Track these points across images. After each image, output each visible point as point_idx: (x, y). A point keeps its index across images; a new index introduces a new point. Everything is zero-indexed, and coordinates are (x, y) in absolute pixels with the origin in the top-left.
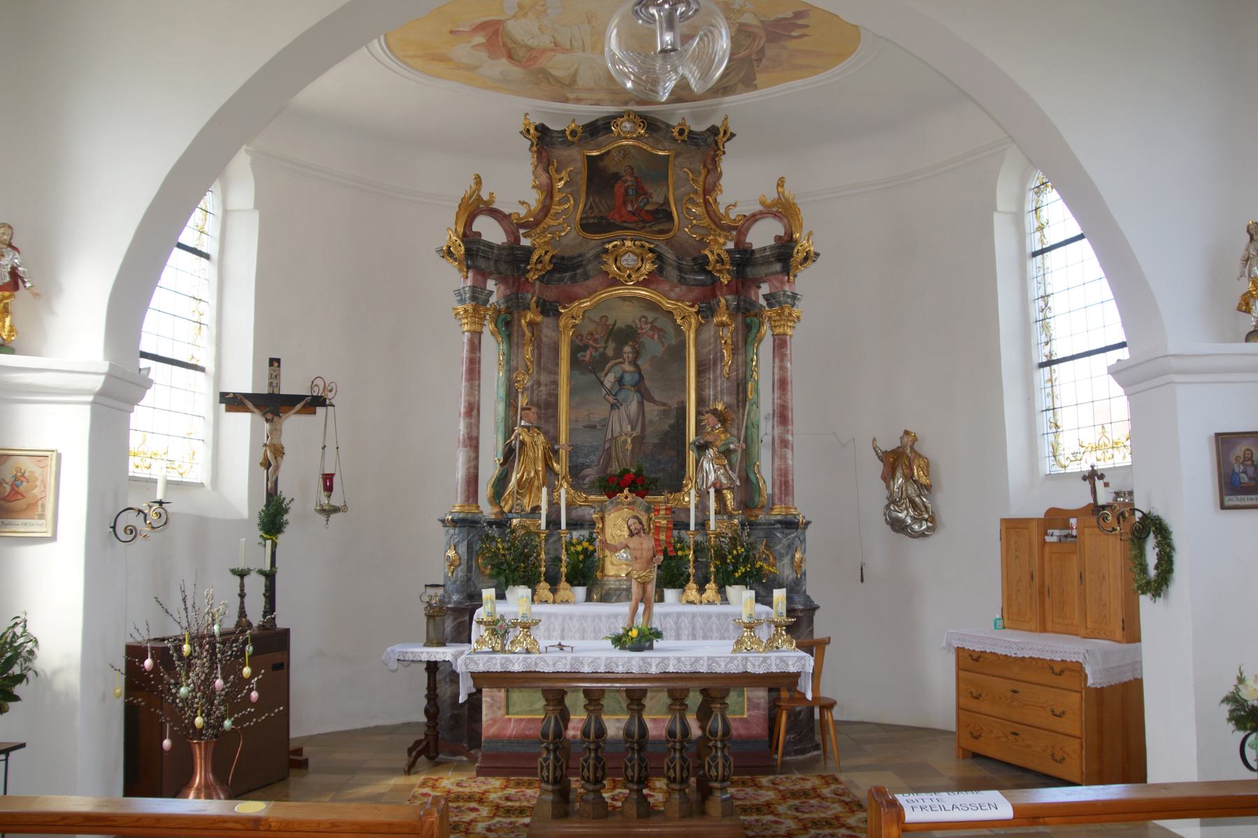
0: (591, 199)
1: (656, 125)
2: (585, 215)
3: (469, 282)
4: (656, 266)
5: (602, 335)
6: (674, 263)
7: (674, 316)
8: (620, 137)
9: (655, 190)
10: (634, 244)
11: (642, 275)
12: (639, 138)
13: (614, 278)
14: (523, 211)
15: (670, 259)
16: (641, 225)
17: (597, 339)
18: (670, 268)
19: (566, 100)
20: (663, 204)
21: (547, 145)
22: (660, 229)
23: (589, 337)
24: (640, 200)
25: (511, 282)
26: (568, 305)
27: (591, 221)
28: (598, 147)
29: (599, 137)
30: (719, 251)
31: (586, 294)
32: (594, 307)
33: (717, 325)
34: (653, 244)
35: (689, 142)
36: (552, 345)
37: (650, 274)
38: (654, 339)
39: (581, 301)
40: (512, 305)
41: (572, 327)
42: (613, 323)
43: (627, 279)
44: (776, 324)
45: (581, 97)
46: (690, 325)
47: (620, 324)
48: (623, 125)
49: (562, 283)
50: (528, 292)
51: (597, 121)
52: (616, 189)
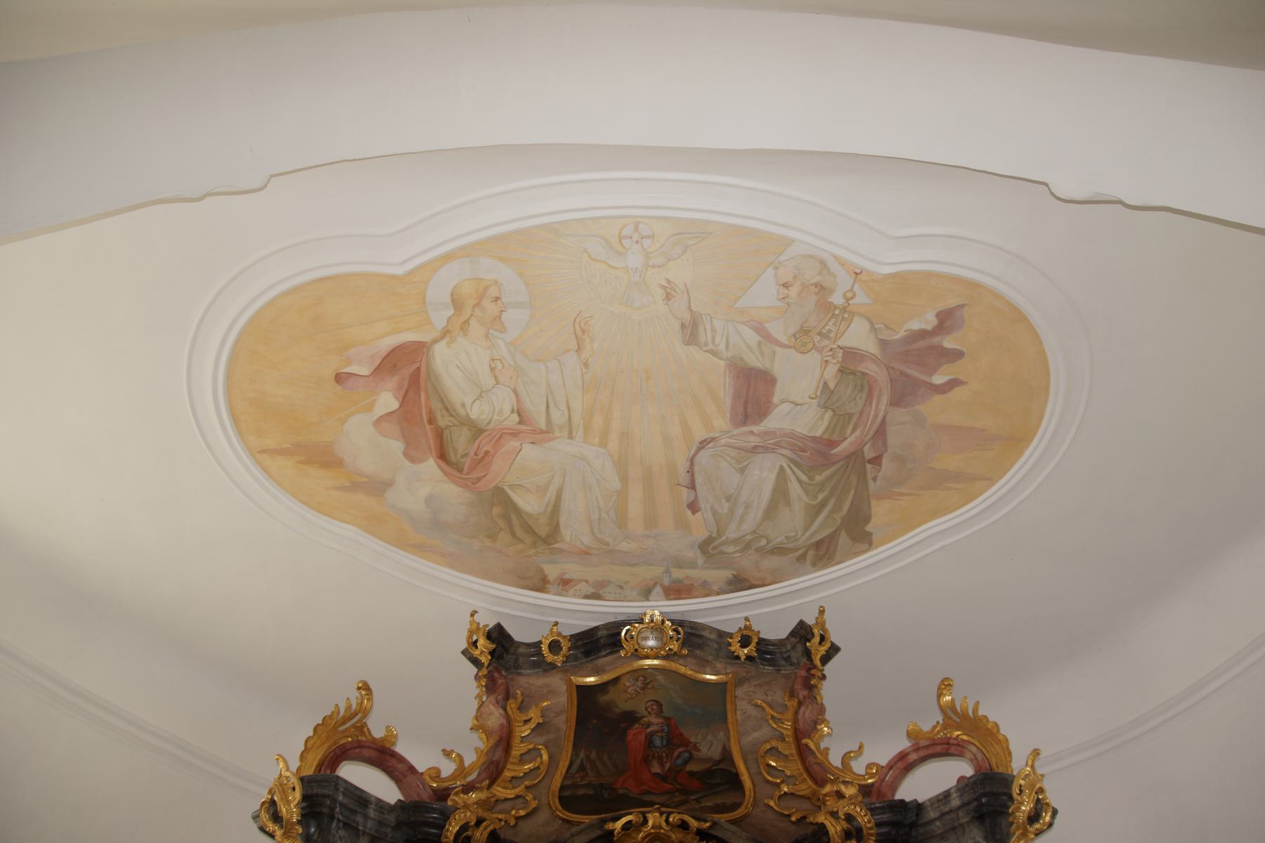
0: (582, 754)
1: (701, 636)
2: (569, 782)
8: (638, 655)
10: (667, 821)
12: (669, 656)
14: (448, 768)
19: (541, 585)
20: (720, 761)
21: (507, 669)
22: (718, 804)
24: (676, 754)
27: (581, 792)
29: (599, 657)
30: (849, 809)
45: (567, 576)
51: (597, 628)
52: (630, 737)
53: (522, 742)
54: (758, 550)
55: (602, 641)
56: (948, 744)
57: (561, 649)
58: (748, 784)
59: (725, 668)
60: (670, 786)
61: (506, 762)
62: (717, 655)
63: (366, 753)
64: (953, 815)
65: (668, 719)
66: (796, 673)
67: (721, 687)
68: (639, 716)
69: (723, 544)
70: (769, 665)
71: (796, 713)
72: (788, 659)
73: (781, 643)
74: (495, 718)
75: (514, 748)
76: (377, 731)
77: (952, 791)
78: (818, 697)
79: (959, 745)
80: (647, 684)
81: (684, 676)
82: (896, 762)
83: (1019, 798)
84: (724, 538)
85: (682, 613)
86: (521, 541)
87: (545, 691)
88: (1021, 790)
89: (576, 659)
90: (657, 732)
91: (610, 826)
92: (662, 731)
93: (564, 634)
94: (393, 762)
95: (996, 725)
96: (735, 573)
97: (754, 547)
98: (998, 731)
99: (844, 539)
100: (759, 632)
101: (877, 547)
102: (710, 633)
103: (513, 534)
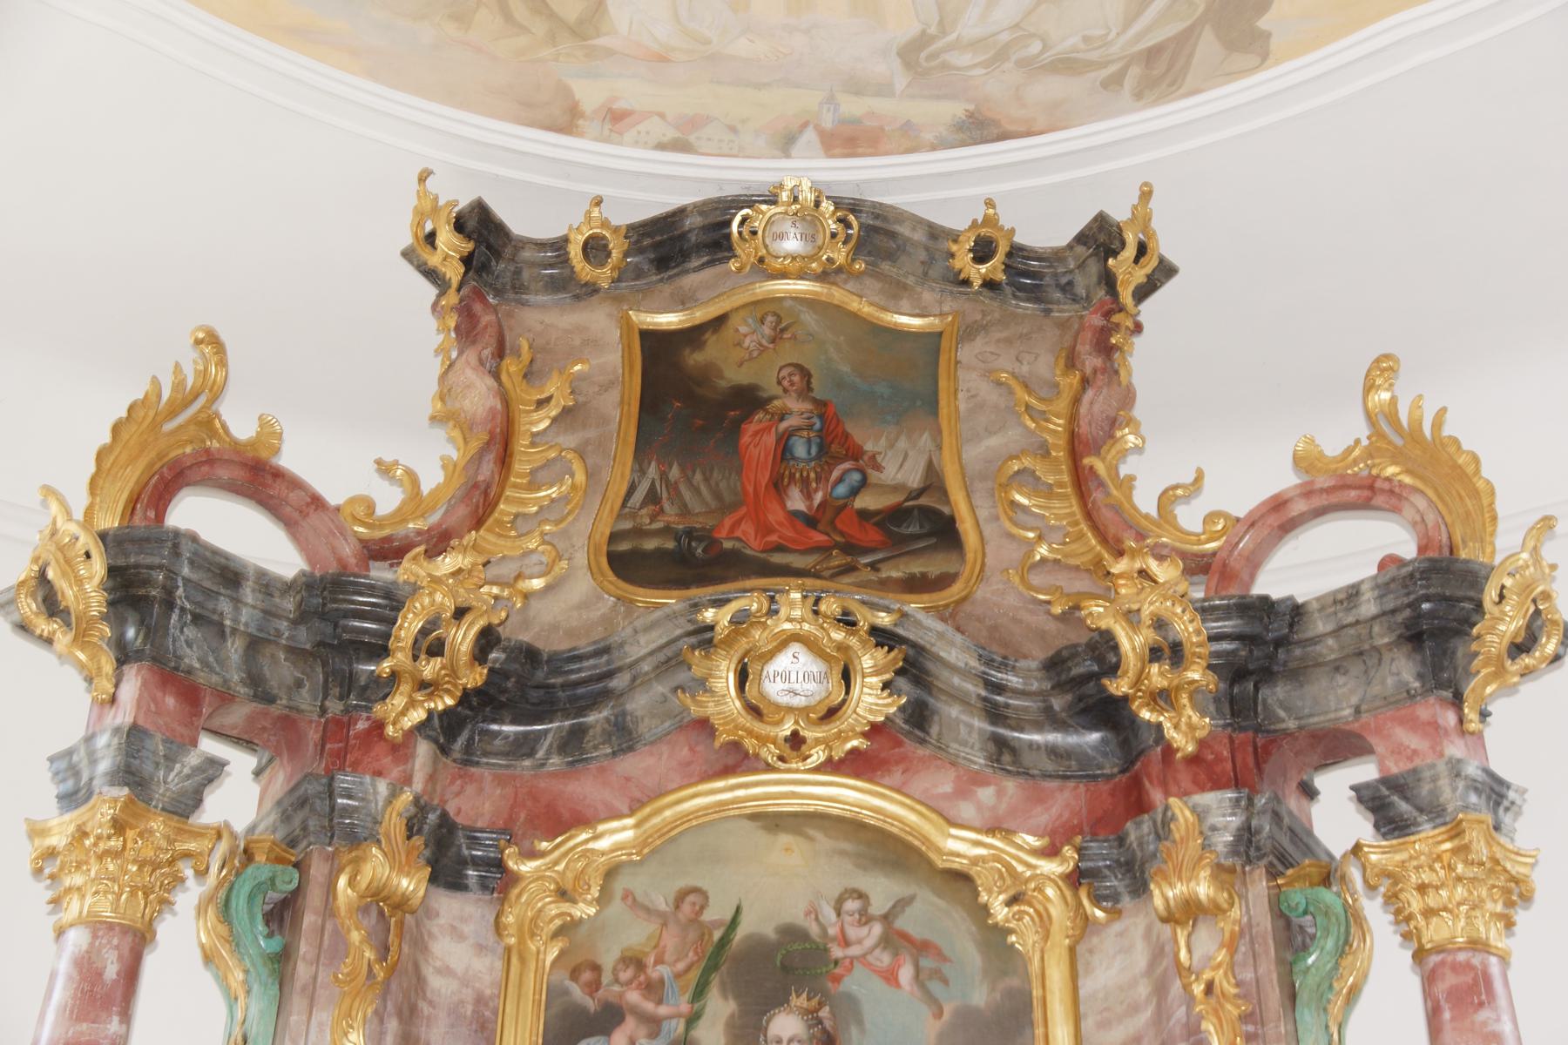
0: (653, 471)
1: (892, 235)
2: (627, 525)
3: (124, 714)
4: (904, 700)
5: (681, 966)
6: (969, 687)
7: (977, 894)
8: (763, 268)
9: (891, 446)
11: (841, 737)
13: (736, 746)
14: (388, 499)
15: (953, 668)
16: (838, 560)
17: (662, 981)
18: (954, 711)
19: (567, 121)
20: (921, 492)
21: (498, 293)
23: (625, 975)
24: (836, 474)
25: (313, 735)
26: (544, 845)
27: (650, 545)
28: (682, 302)
29: (687, 272)
31: (626, 810)
32: (654, 849)
33: (1169, 919)
34: (888, 610)
35: (1008, 290)
36: (469, 1009)
37: (875, 731)
38: (897, 985)
39: (601, 828)
40: (305, 828)
41: (556, 934)
42: (728, 916)
43: (787, 752)
44: (1432, 900)
45: (621, 105)
46: (1044, 920)
47: (758, 923)
48: (776, 229)
49: (527, 763)
50: (379, 773)
51: (680, 213)
52: (745, 439)
53: (533, 445)
54: (1023, 63)
55: (693, 238)
56: (1371, 488)
57: (609, 255)
58: (970, 538)
59: (941, 303)
60: (823, 538)
61: (503, 484)
62: (926, 274)
63: (224, 473)
64: (1363, 630)
65: (821, 405)
66: (1082, 317)
67: (931, 342)
68: (765, 395)
69: (951, 48)
70: (1028, 300)
71: (1076, 401)
72: (1067, 288)
73: (1056, 256)
74: (478, 396)
75: (517, 457)
76: (240, 423)
77: (1364, 587)
78: (1123, 373)
79: (1391, 492)
80: (782, 331)
81: (855, 316)
82: (1262, 516)
83: (1496, 610)
84: (952, 37)
85: (858, 184)
86: (524, 30)
87: (577, 342)
88: (1502, 597)
89: (639, 274)
90: (800, 429)
91: (709, 615)
92: (810, 427)
93: (615, 222)
94: (278, 489)
95: (1476, 460)
96: (971, 107)
97: (1014, 58)
98: (1477, 471)
99: (1208, 45)
100: (1013, 231)
101: (1277, 63)
102: (914, 229)
103: (508, 17)
